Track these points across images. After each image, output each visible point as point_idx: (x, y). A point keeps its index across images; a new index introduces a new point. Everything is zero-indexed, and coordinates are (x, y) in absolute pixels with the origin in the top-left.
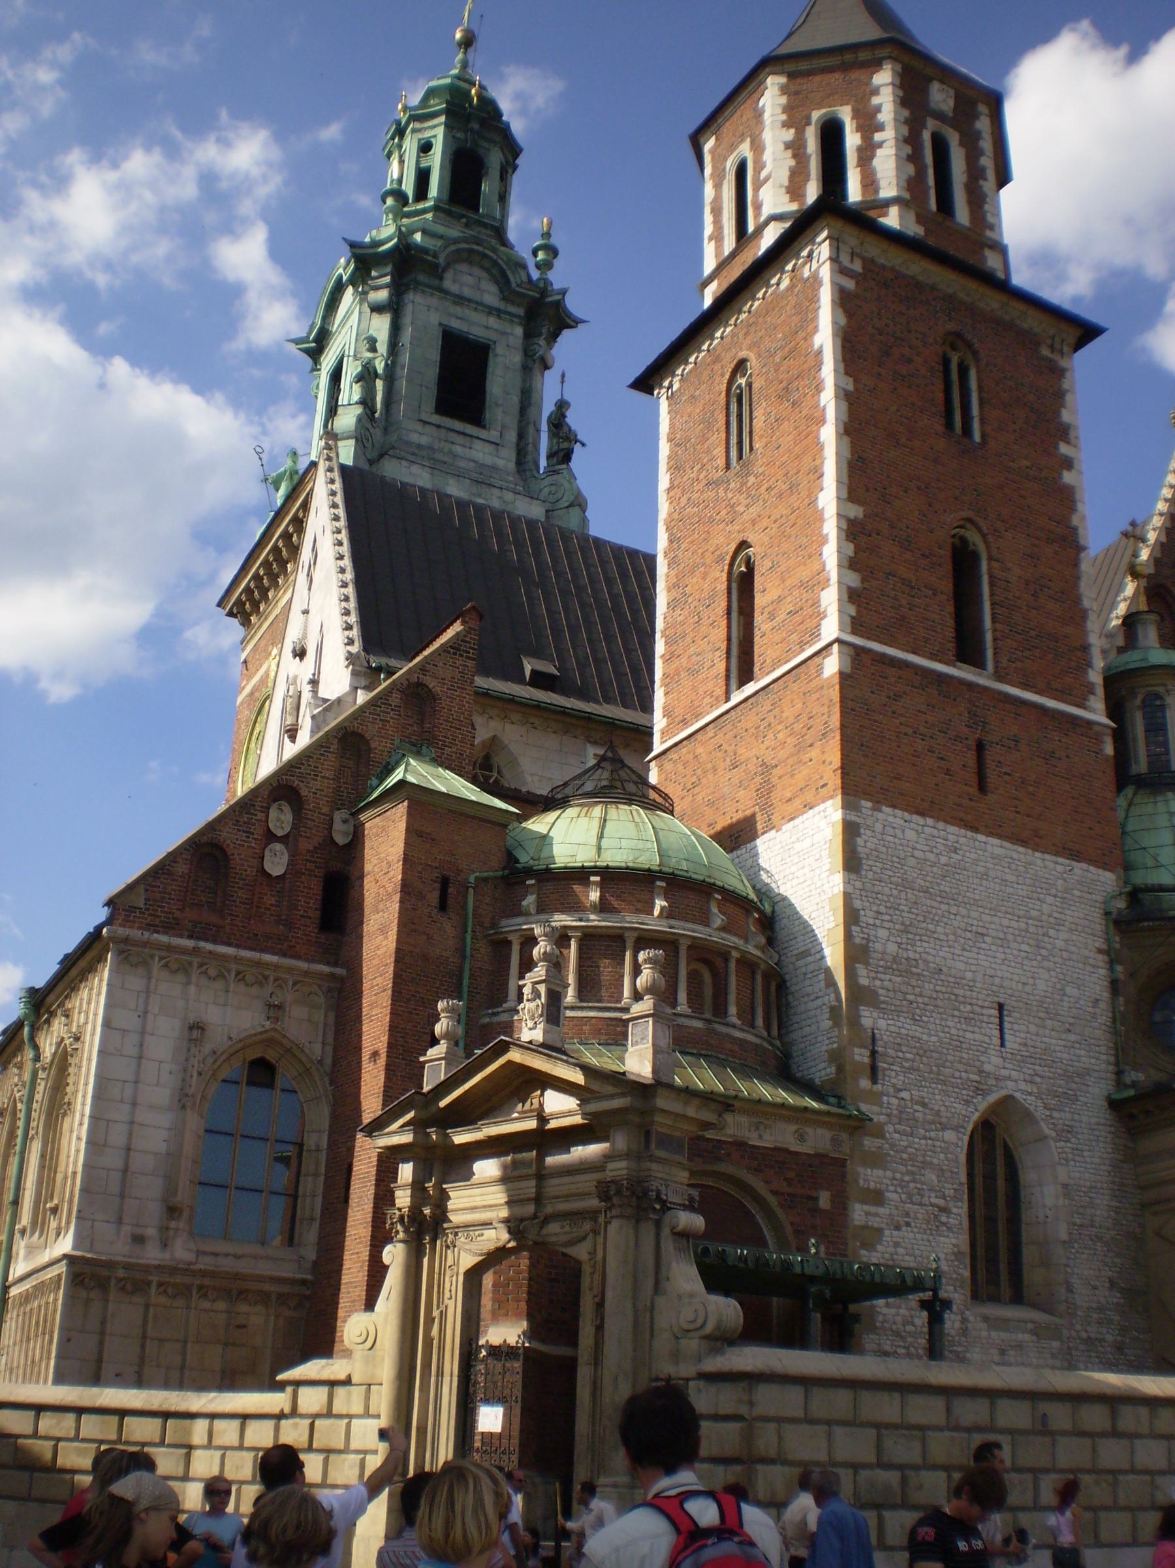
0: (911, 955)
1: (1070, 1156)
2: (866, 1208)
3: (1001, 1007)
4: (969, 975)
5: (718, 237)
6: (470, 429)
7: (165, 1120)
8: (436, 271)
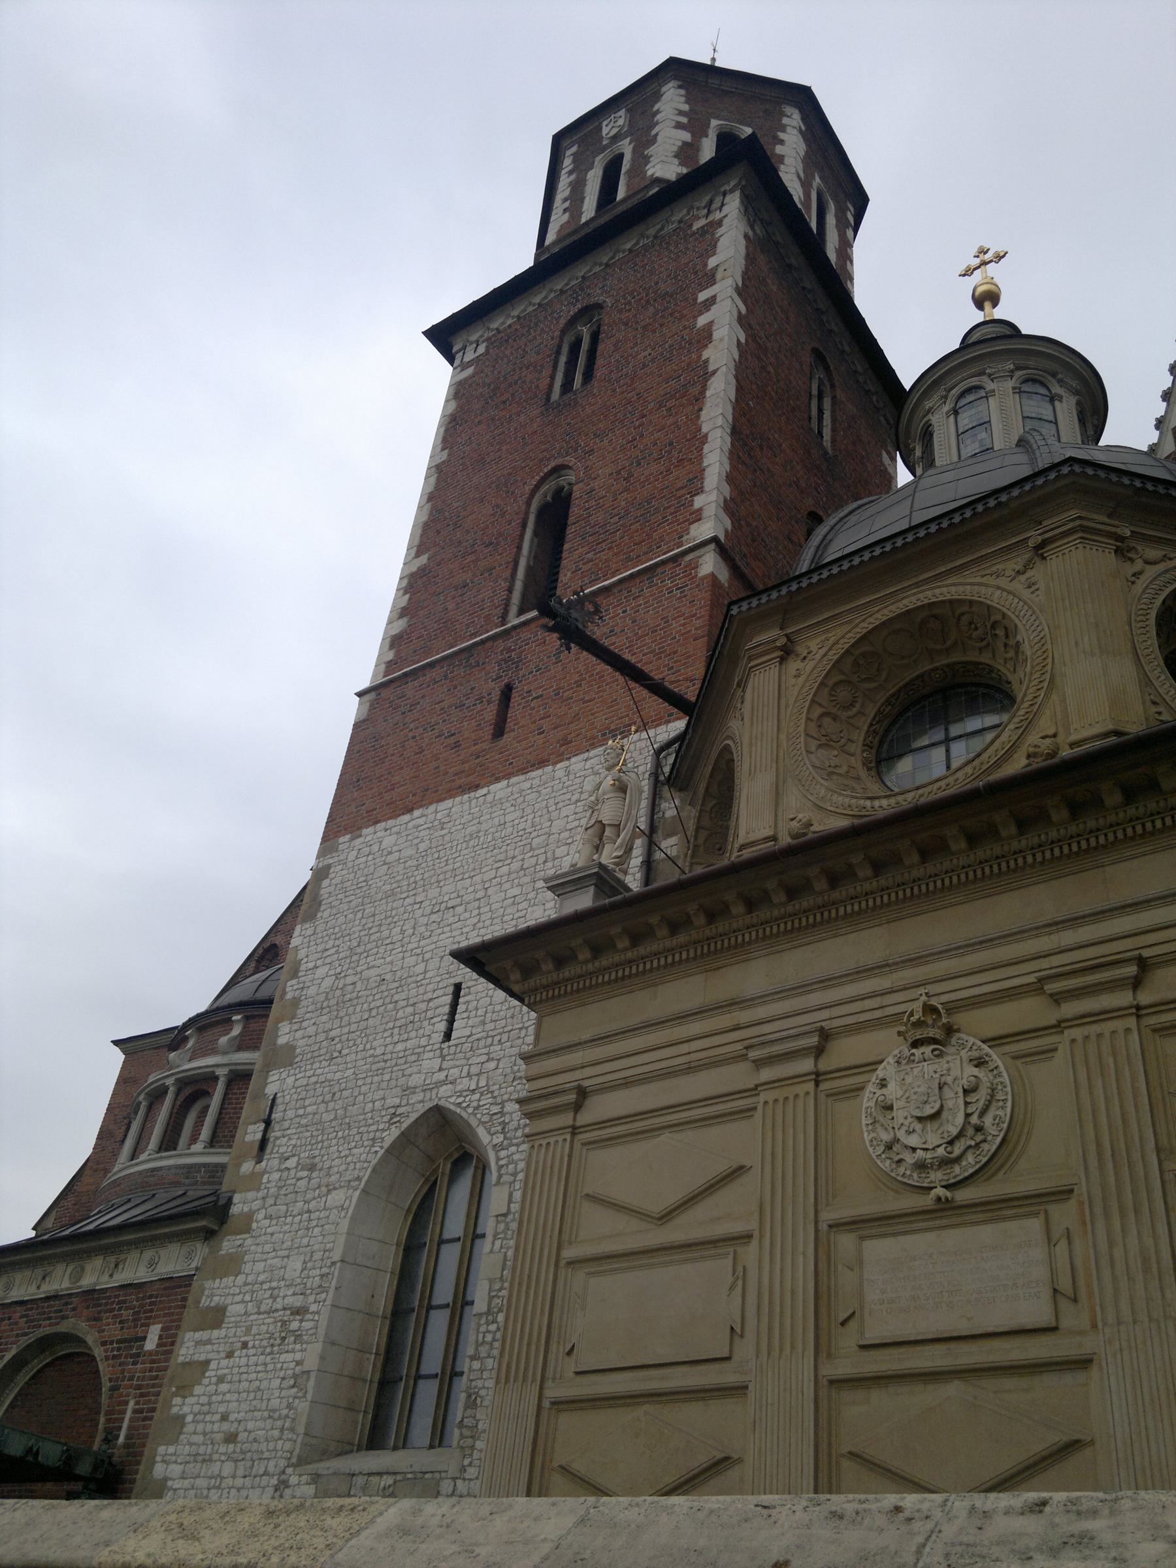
2: (198, 1335)
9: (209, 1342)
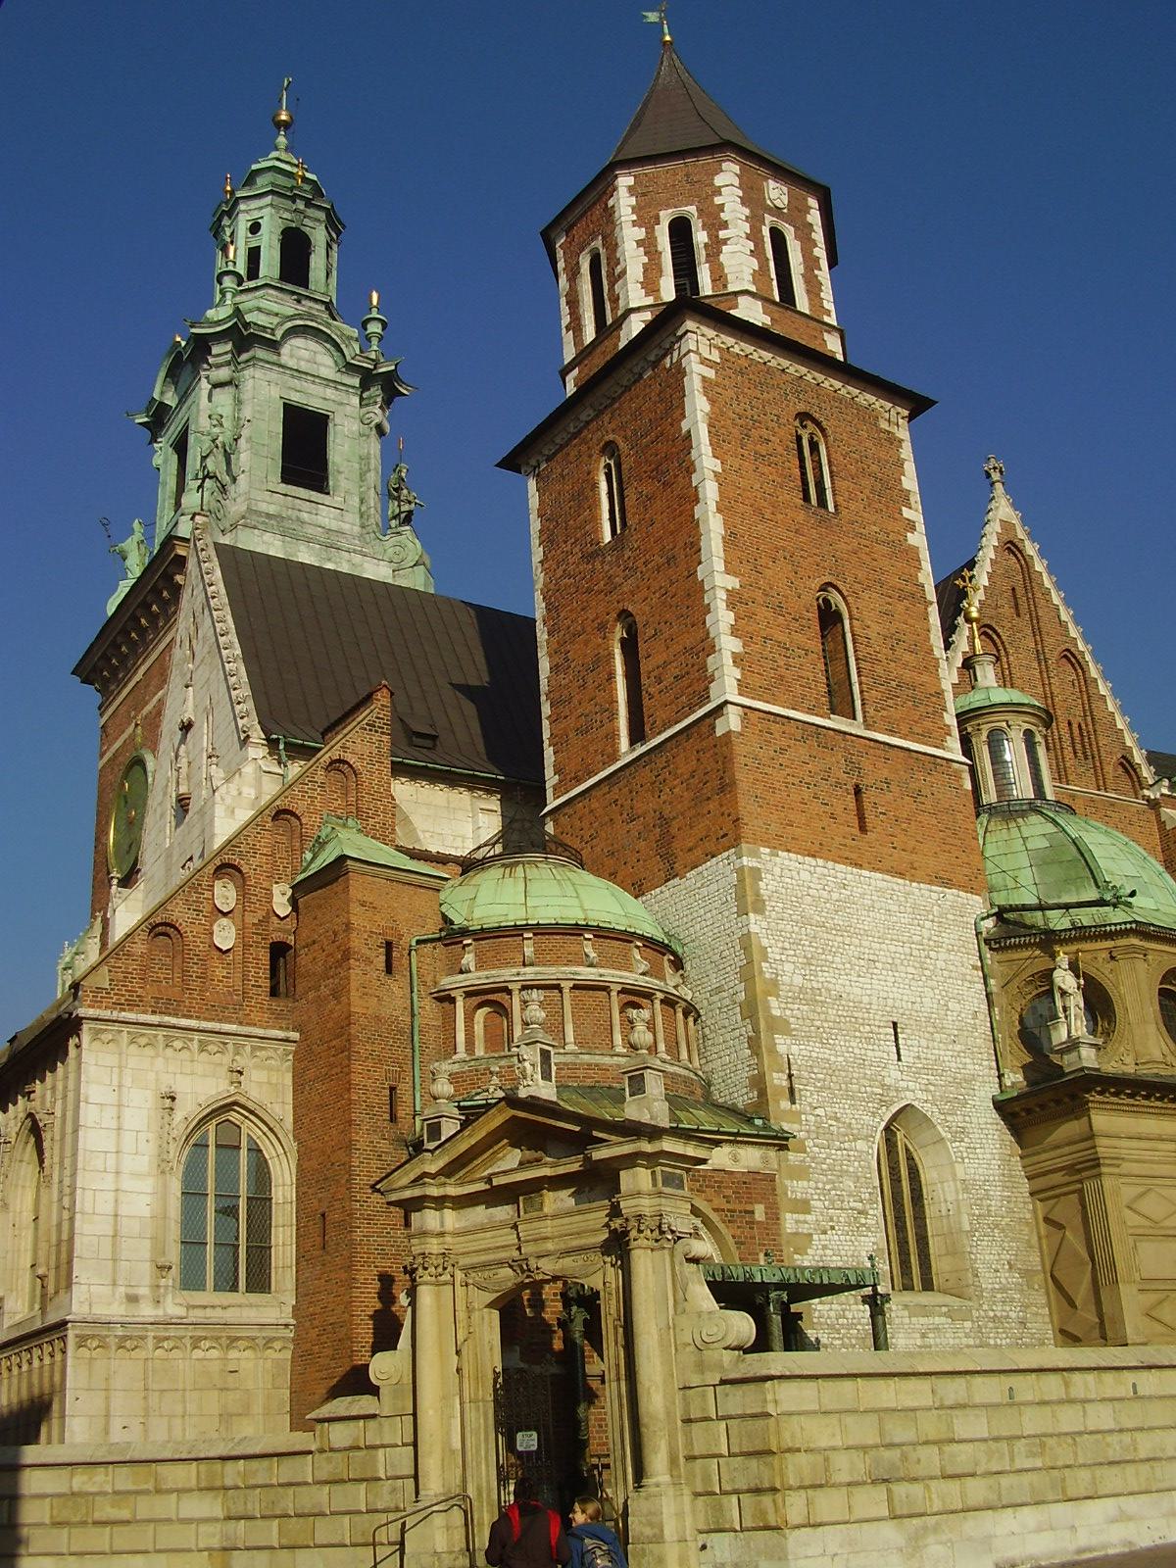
0: (815, 985)
1: (965, 1155)
3: (895, 1024)
4: (866, 999)
5: (576, 326)
6: (315, 495)
7: (148, 1185)
8: (274, 346)
9: (806, 1222)
